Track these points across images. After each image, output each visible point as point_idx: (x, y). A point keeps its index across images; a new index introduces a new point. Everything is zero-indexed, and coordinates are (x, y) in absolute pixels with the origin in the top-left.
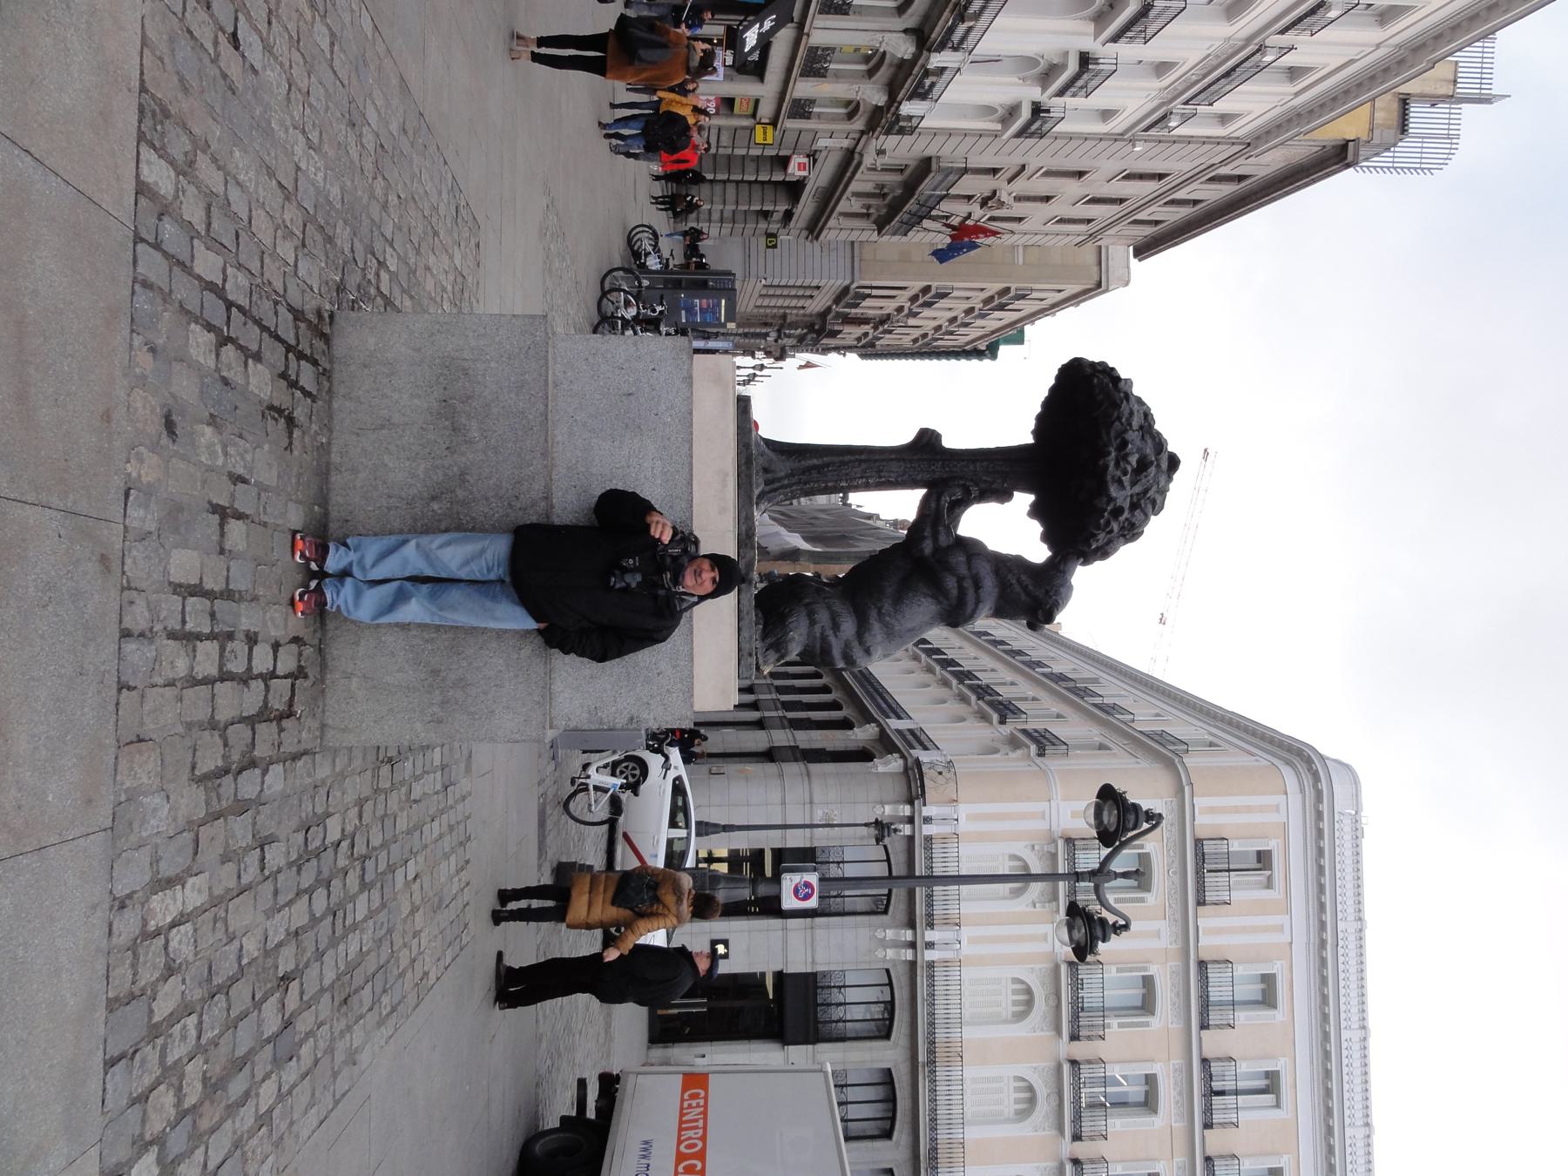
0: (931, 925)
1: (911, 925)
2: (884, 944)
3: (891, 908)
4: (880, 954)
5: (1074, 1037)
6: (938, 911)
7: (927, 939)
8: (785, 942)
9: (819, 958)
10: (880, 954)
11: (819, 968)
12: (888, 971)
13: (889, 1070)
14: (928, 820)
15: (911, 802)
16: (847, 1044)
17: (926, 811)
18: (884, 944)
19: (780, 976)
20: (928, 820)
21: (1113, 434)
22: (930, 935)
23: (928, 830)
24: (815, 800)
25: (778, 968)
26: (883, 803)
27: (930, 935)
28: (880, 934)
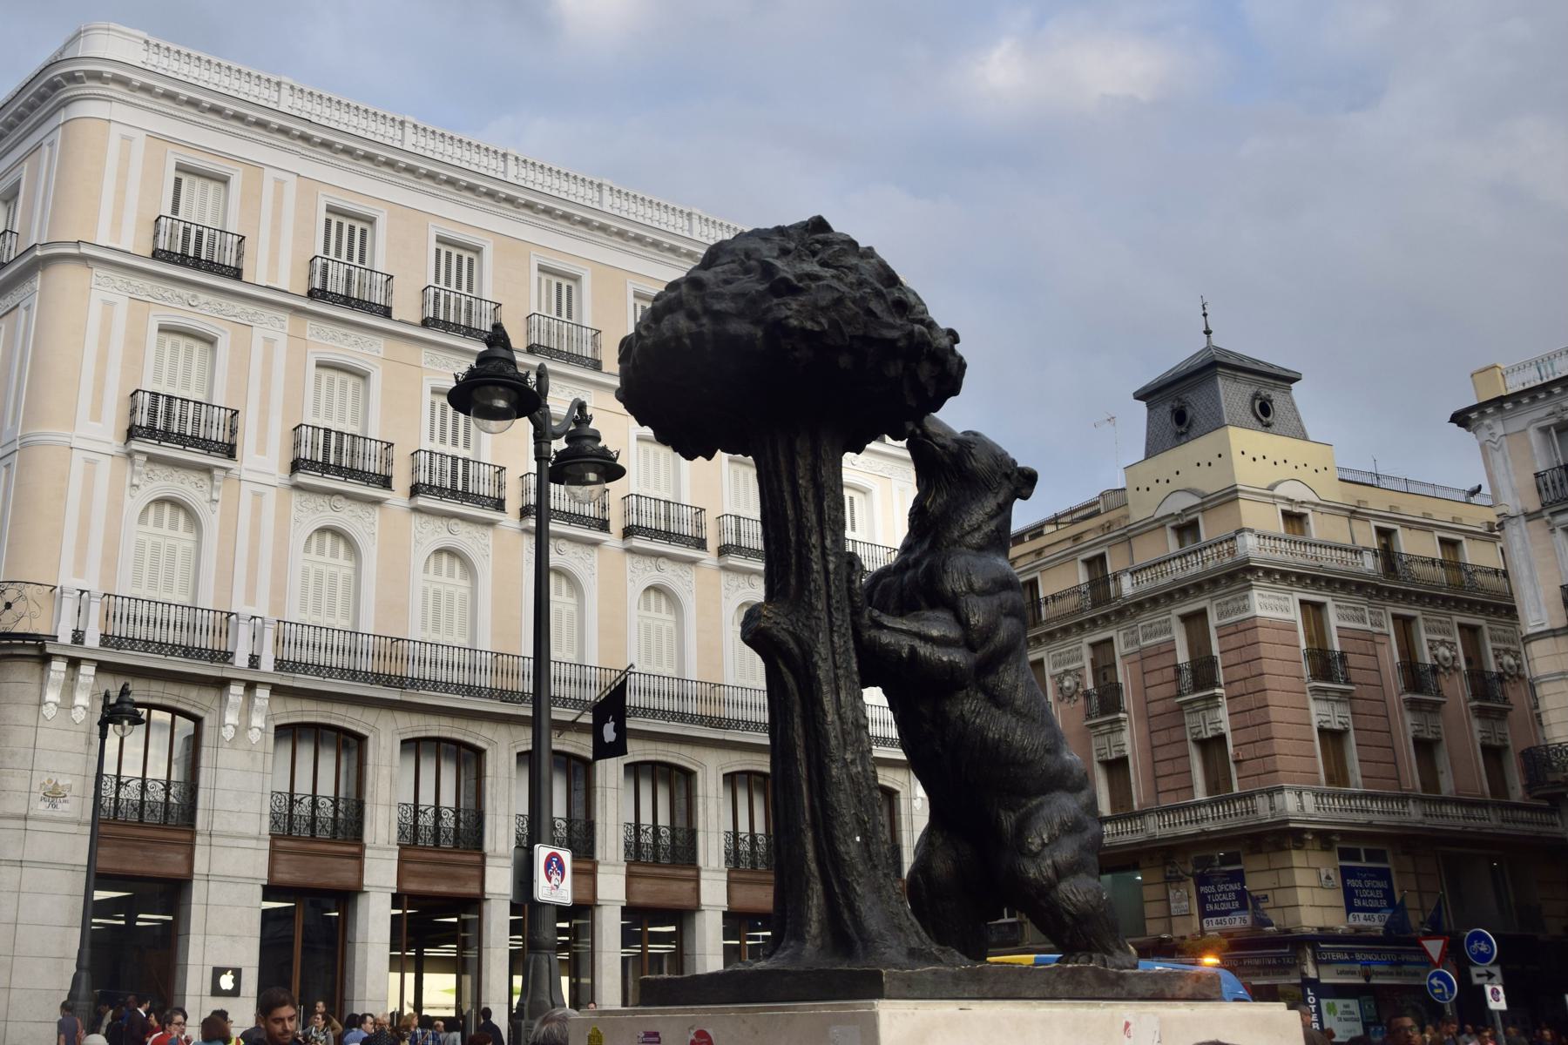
0: (226, 657)
1: (222, 684)
2: (243, 728)
3: (194, 711)
4: (255, 736)
5: (386, 482)
6: (204, 641)
7: (246, 664)
8: (227, 879)
9: (254, 831)
10: (255, 736)
11: (266, 829)
12: (278, 728)
13: (403, 742)
14: (78, 637)
15: (45, 659)
16: (368, 799)
17: (65, 637)
18: (243, 728)
19: (269, 892)
20: (78, 637)
21: (891, 320)
22: (241, 660)
23: (92, 640)
24: (23, 811)
25: (259, 891)
26: (41, 703)
27: (241, 660)
28: (228, 733)
